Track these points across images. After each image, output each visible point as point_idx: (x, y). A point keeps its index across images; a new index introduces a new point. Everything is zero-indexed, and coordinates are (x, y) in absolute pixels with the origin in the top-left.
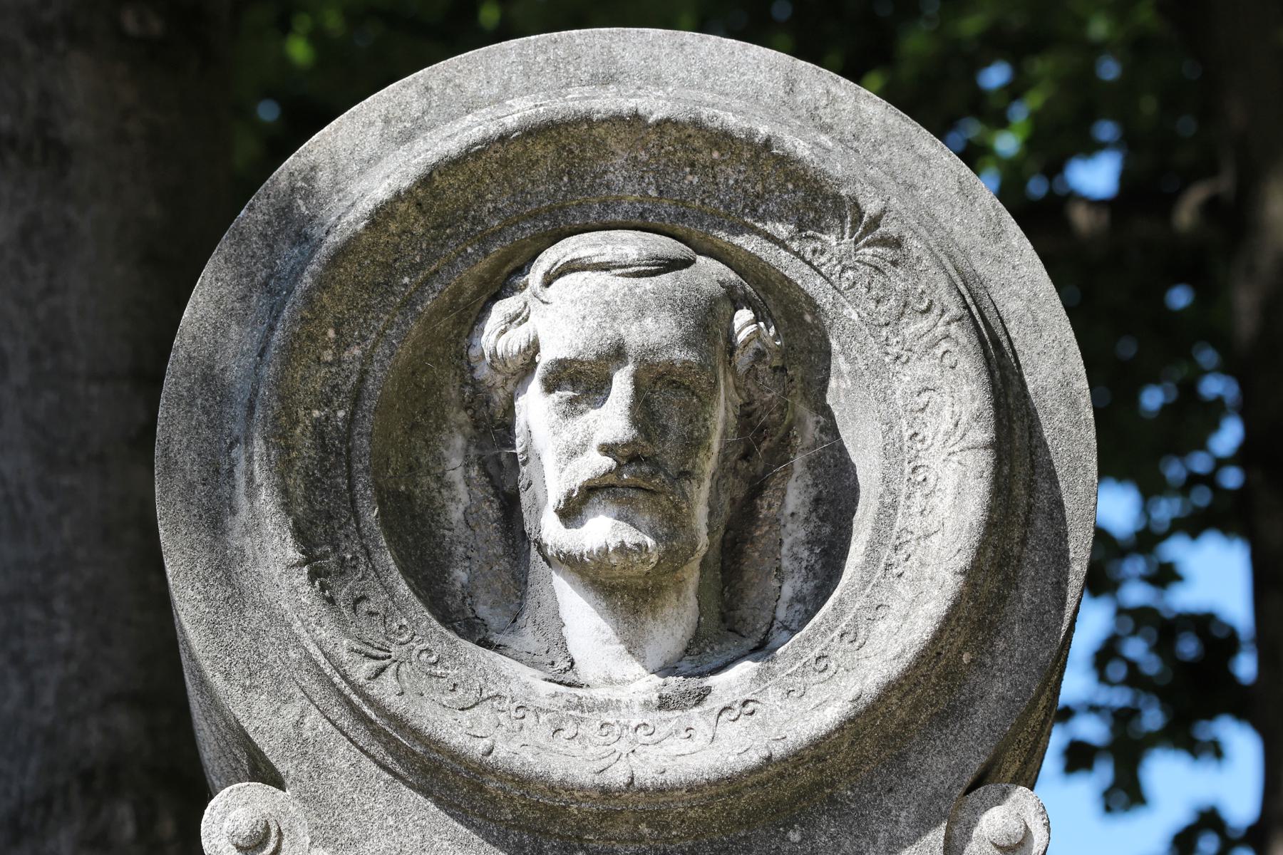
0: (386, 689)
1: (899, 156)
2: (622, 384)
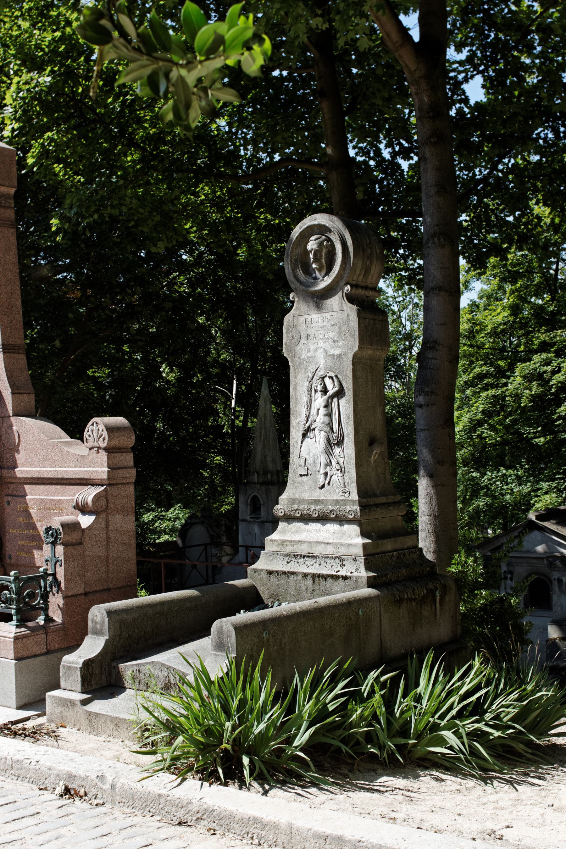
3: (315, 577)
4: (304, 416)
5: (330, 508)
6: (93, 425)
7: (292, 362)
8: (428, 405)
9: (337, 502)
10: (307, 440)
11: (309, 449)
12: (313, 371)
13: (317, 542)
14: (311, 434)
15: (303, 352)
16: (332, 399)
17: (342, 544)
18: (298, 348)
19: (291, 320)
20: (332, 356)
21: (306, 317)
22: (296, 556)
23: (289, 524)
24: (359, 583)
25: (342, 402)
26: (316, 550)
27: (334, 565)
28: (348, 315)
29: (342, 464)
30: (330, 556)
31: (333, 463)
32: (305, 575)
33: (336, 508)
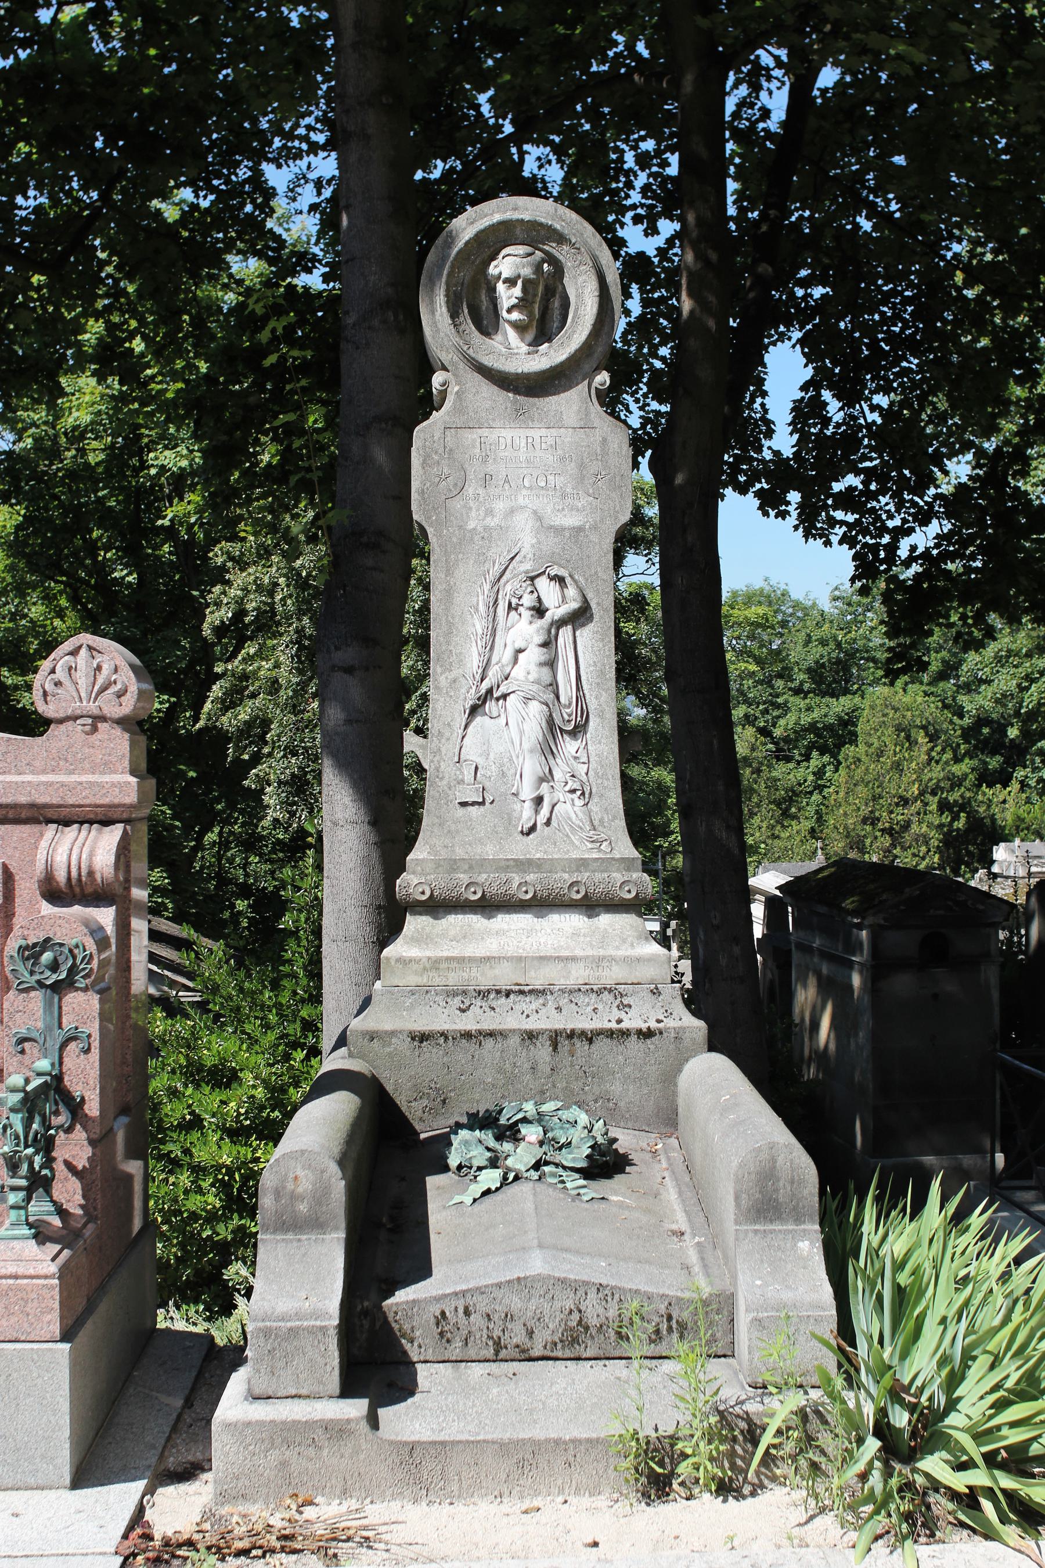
0: (471, 352)
1: (578, 226)
2: (520, 283)
3: (555, 1038)
4: (474, 662)
5: (568, 878)
6: (74, 653)
7: (440, 536)
8: (367, 669)
9: (582, 864)
10: (478, 720)
11: (487, 743)
12: (504, 561)
13: (542, 958)
14: (491, 706)
15: (473, 514)
16: (558, 629)
17: (613, 959)
18: (457, 504)
19: (437, 435)
20: (558, 530)
21: (485, 432)
22: (483, 994)
23: (436, 918)
24: (687, 1042)
25: (586, 635)
26: (537, 979)
27: (600, 1007)
28: (604, 440)
29: (584, 778)
30: (583, 988)
31: (558, 775)
32: (531, 1036)
33: (584, 876)
